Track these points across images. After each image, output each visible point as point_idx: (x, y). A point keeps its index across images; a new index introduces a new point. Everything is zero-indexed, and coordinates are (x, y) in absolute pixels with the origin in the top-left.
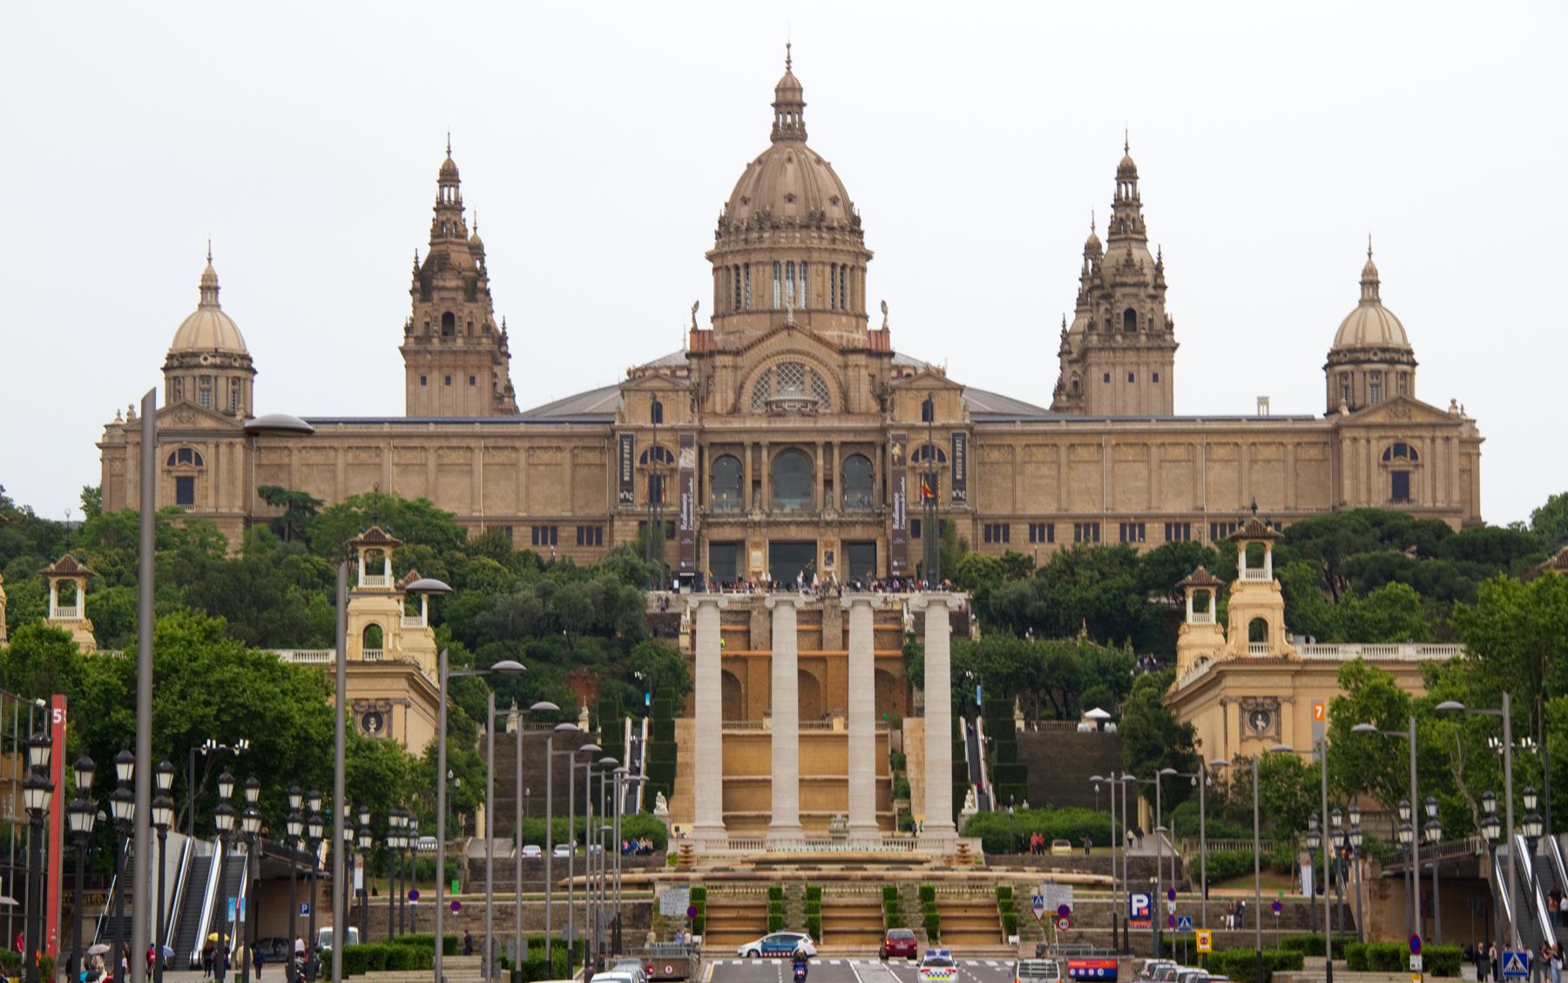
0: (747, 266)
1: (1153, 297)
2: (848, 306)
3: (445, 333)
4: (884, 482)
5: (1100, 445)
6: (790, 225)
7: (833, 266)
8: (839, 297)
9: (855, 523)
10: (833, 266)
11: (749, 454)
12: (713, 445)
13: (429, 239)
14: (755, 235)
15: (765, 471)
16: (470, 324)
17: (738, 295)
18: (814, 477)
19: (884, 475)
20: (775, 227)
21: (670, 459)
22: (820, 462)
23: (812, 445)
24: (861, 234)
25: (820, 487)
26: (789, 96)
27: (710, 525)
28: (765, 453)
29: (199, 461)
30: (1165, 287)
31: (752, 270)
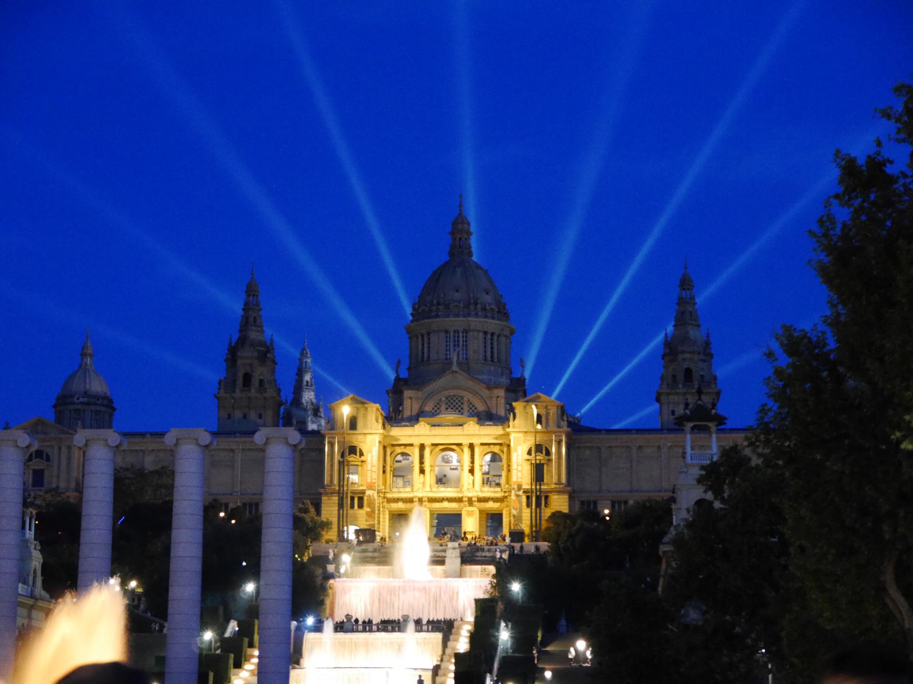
0: (429, 334)
5: (659, 447)
10: (485, 333)
12: (393, 445)
16: (261, 381)
17: (423, 353)
23: (459, 445)
27: (390, 501)
29: (48, 459)
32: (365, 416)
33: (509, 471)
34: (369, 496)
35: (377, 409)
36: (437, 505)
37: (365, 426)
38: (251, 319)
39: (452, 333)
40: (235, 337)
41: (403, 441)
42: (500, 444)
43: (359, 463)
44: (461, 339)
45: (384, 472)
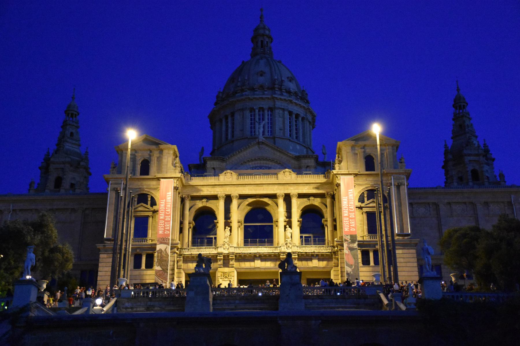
0: (233, 114)
1: (488, 164)
2: (301, 140)
3: (55, 188)
6: (262, 87)
7: (290, 113)
8: (294, 136)
9: (313, 255)
10: (290, 113)
14: (239, 94)
16: (72, 185)
17: (227, 135)
20: (253, 89)
23: (273, 197)
24: (307, 102)
26: (261, 31)
30: (494, 160)
32: (160, 159)
33: (335, 228)
34: (161, 250)
35: (175, 153)
36: (247, 265)
37: (159, 170)
38: (68, 133)
41: (206, 191)
43: (150, 214)
44: (266, 117)
45: (181, 230)
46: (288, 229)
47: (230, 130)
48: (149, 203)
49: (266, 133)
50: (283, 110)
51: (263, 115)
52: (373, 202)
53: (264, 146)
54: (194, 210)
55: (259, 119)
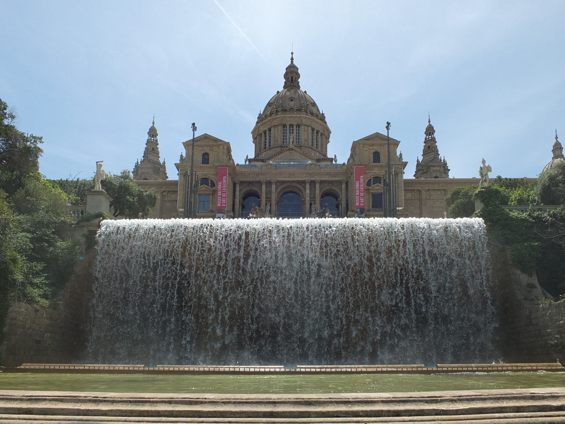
0: (270, 130)
4: (347, 204)
10: (313, 130)
11: (264, 187)
12: (241, 183)
13: (143, 155)
15: (274, 196)
17: (265, 145)
18: (304, 203)
19: (347, 200)
20: (284, 111)
21: (213, 185)
22: (308, 192)
24: (325, 122)
25: (308, 206)
28: (274, 186)
31: (272, 129)
39: (288, 127)
40: (140, 157)
42: (340, 182)
44: (295, 131)
46: (313, 206)
47: (267, 141)
48: (210, 184)
49: (295, 143)
50: (308, 126)
51: (293, 130)
52: (378, 186)
53: (293, 152)
54: (242, 192)
55: (290, 133)
